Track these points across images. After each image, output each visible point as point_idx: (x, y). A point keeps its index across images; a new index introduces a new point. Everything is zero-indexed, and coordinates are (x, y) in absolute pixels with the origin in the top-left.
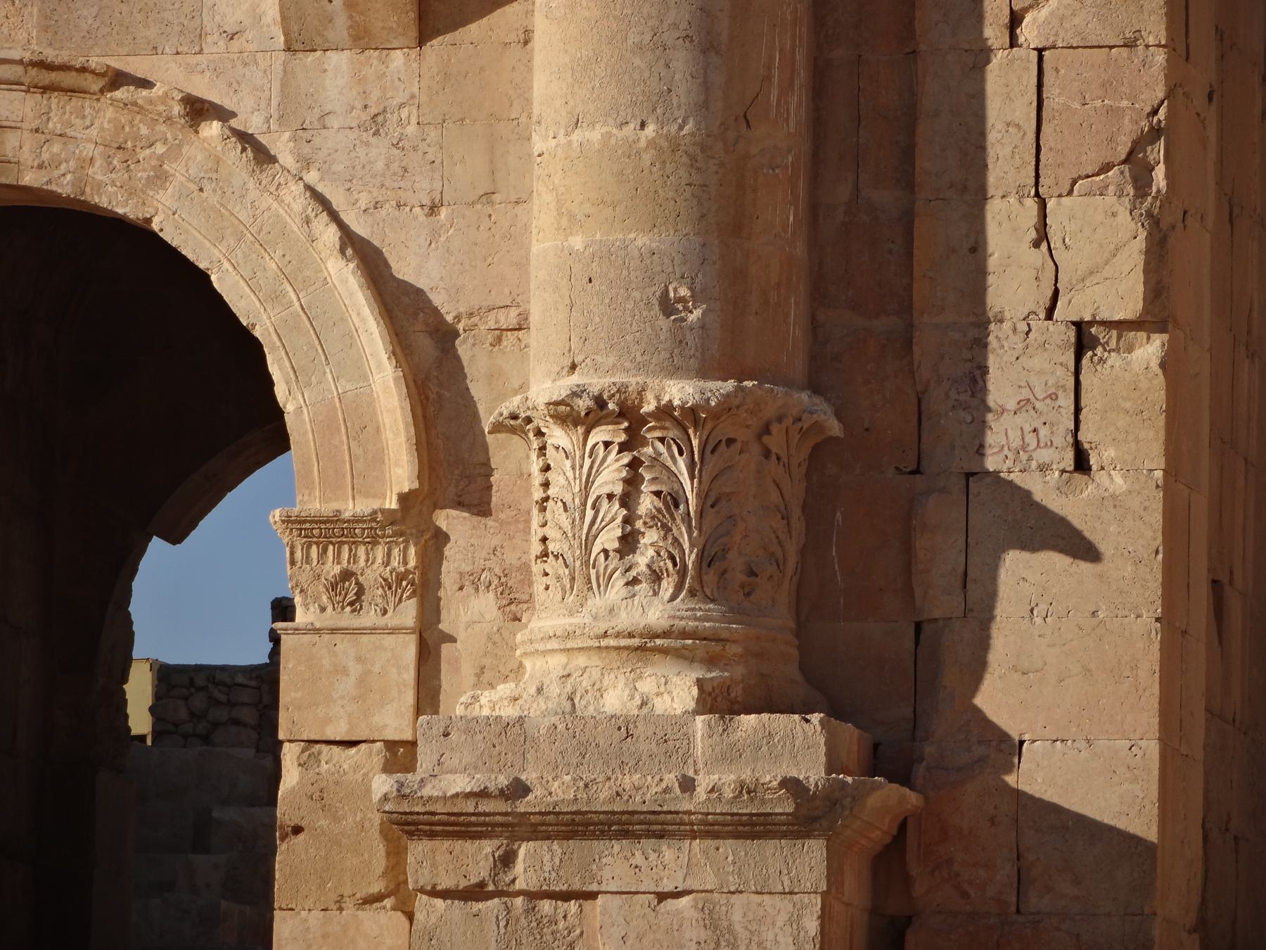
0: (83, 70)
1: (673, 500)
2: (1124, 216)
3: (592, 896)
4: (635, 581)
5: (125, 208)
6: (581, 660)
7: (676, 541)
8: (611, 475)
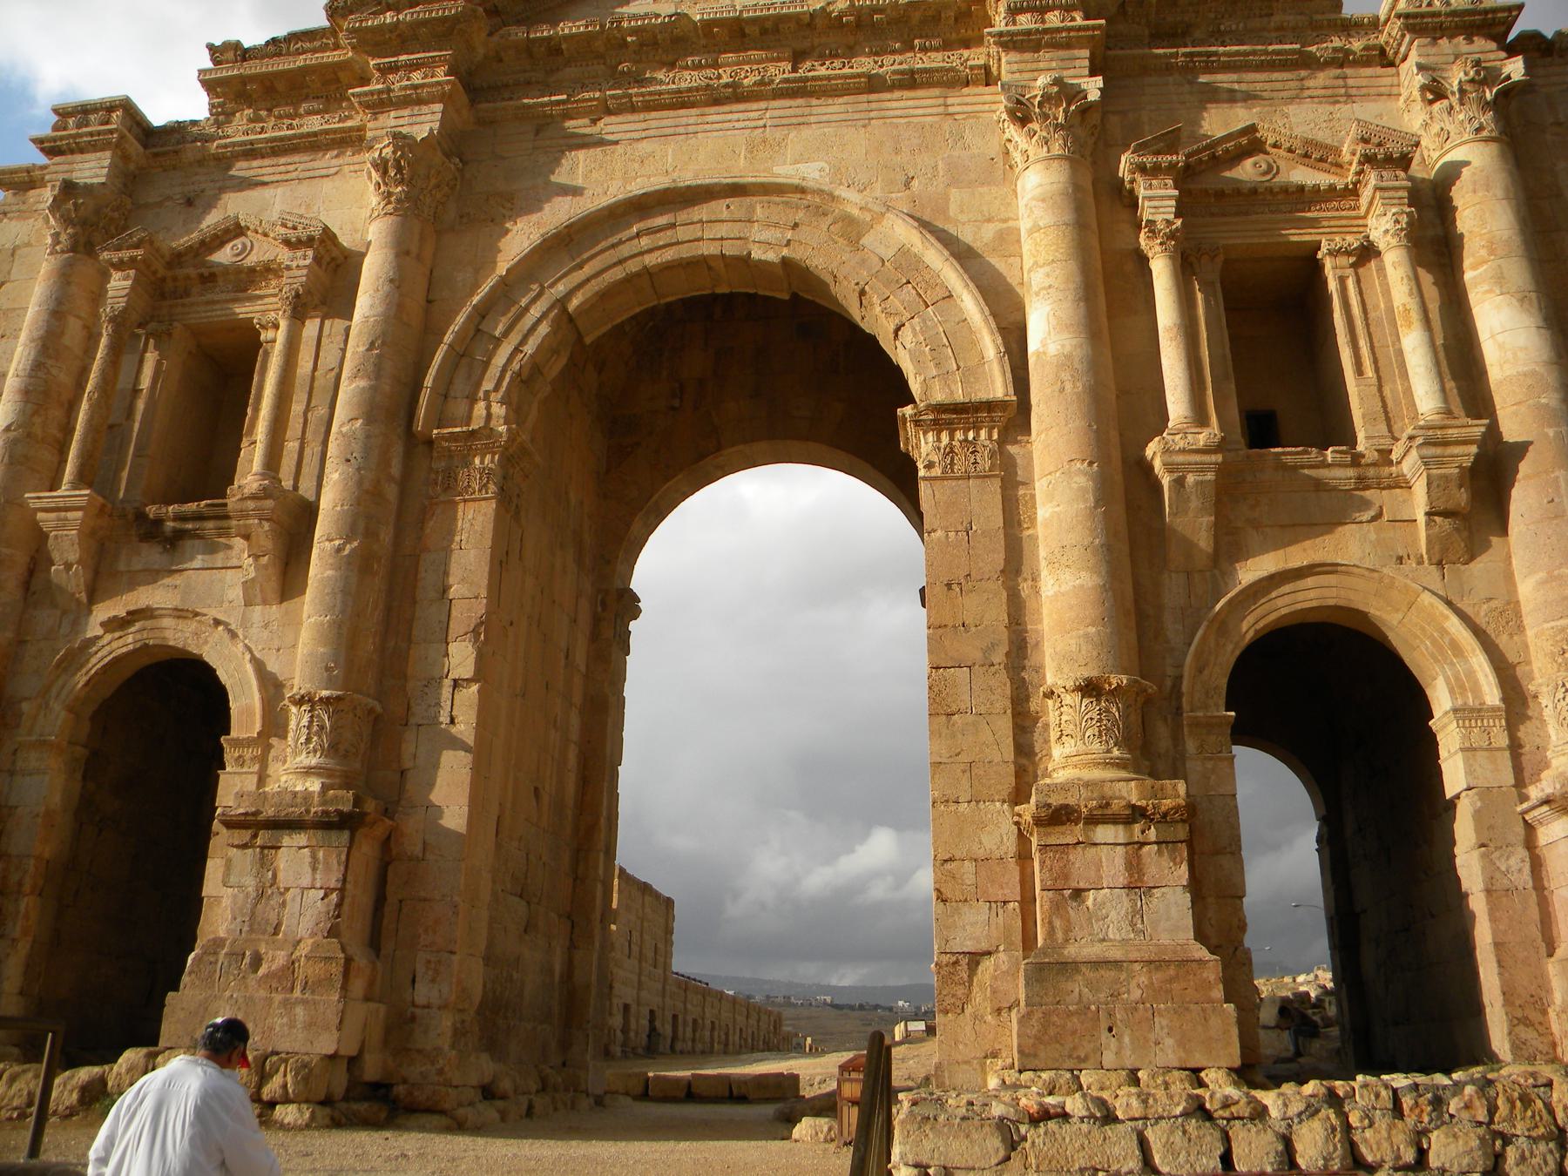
0: (187, 610)
1: (322, 727)
2: (470, 648)
3: (280, 847)
4: (309, 753)
6: (291, 777)
7: (322, 741)
8: (305, 721)
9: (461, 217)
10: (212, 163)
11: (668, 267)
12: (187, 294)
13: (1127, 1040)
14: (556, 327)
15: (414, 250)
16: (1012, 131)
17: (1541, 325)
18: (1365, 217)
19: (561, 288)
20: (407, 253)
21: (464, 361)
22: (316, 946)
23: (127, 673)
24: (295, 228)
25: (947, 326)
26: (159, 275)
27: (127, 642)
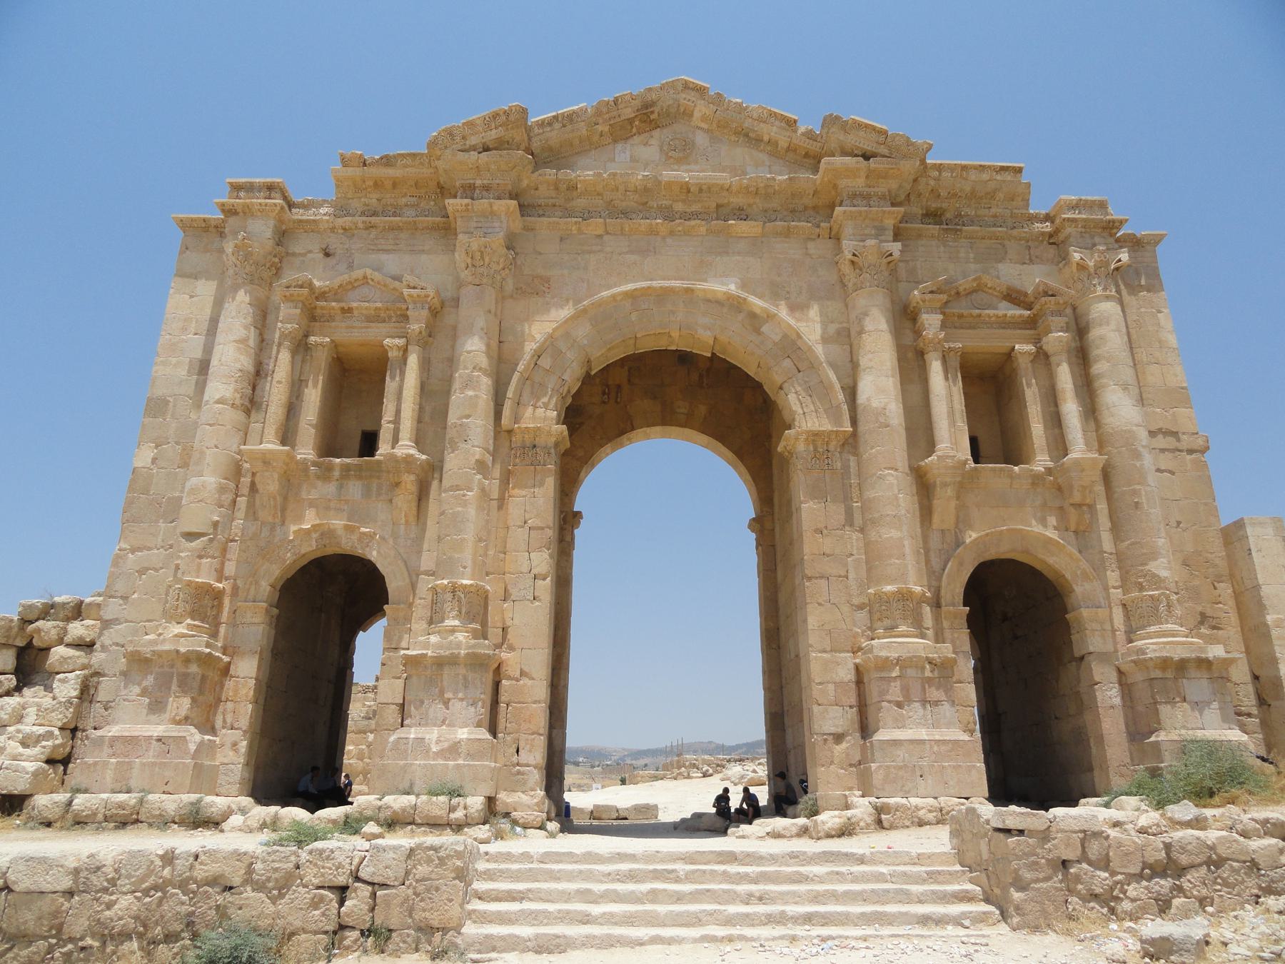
5: (359, 551)
10: (341, 231)
12: (331, 318)
13: (930, 781)
15: (493, 311)
16: (847, 269)
20: (490, 312)
21: (528, 382)
22: (469, 733)
24: (414, 288)
26: (313, 306)
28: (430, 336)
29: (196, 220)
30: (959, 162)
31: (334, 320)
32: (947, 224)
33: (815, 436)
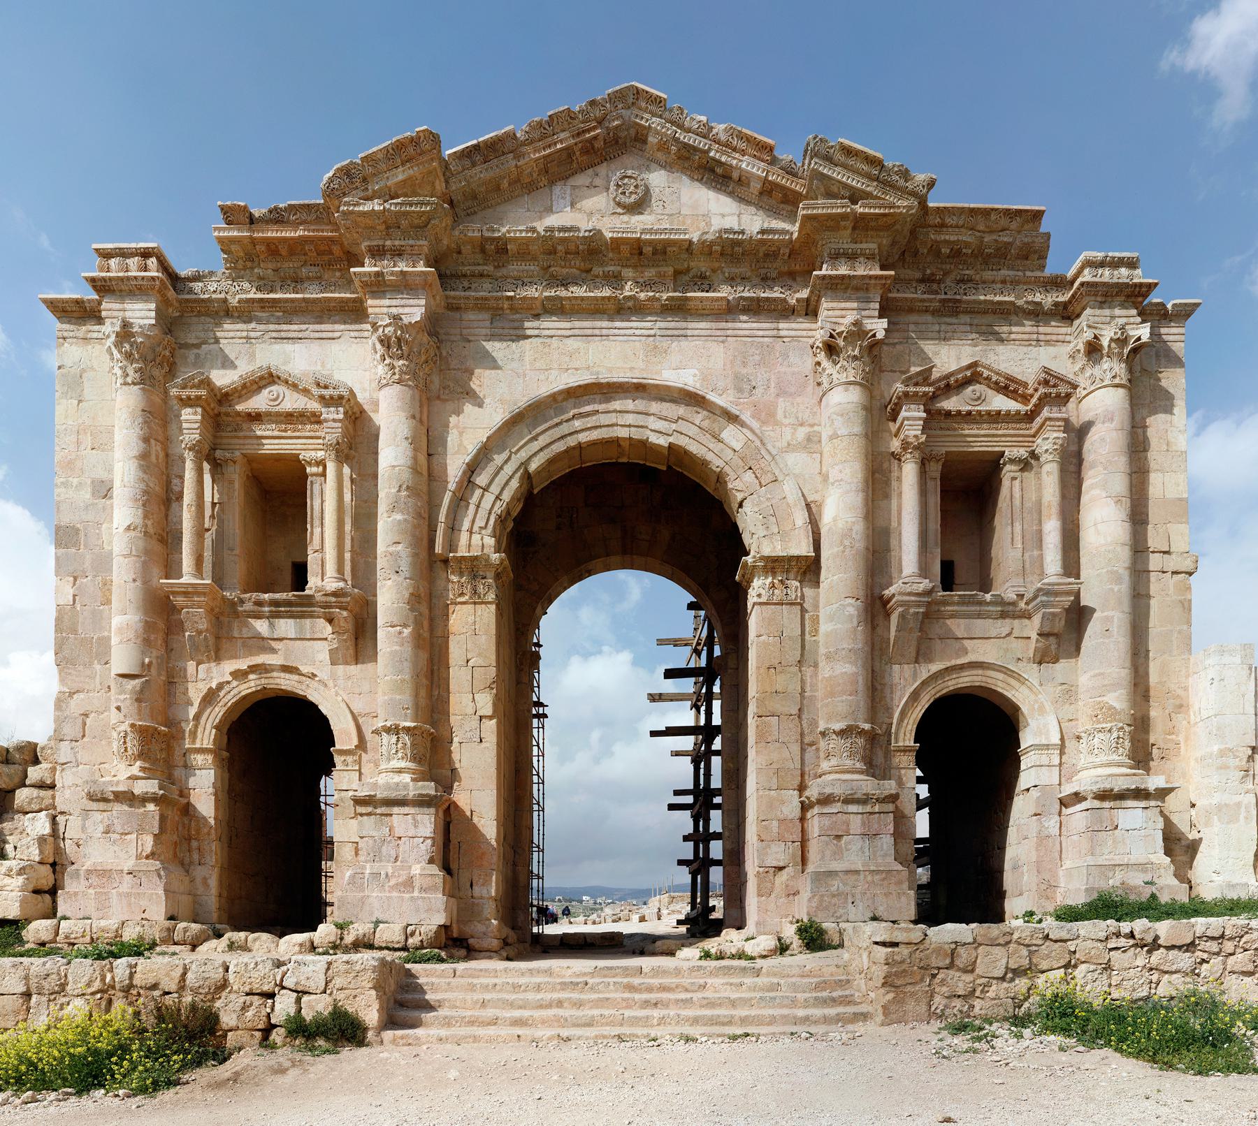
5: (301, 693)
9: (444, 388)
11: (594, 444)
14: (521, 478)
16: (822, 356)
17: (1125, 519)
18: (1034, 436)
19: (523, 455)
21: (463, 503)
23: (247, 705)
25: (774, 501)
27: (252, 685)
28: (351, 449)
29: (67, 302)
30: (966, 205)
31: (241, 430)
32: (946, 293)
33: (774, 565)
